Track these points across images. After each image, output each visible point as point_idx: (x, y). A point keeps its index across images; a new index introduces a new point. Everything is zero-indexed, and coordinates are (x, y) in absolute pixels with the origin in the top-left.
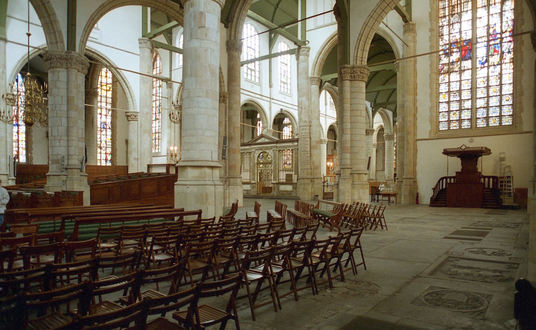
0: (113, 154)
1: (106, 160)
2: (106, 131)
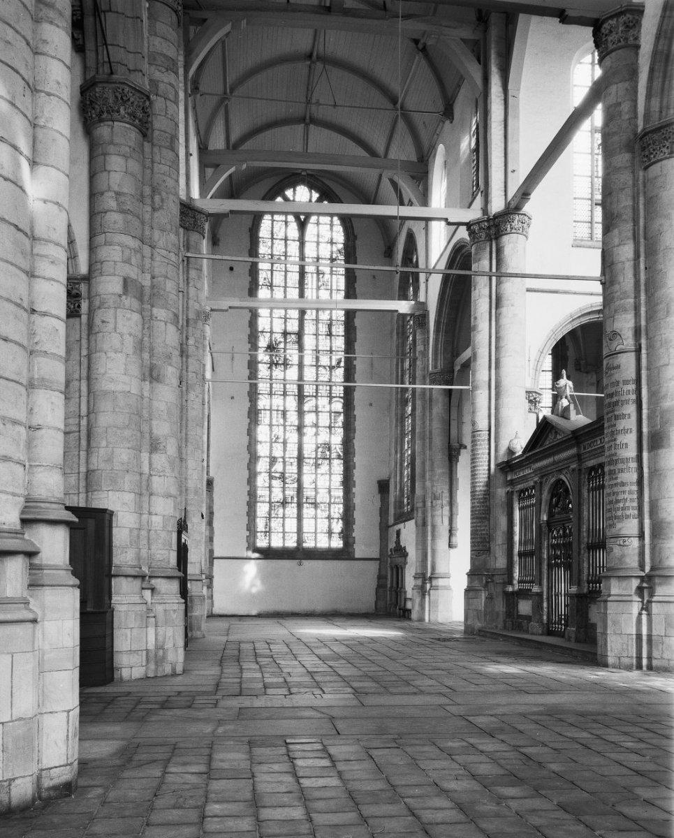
0: (348, 518)
1: (330, 533)
2: (330, 464)
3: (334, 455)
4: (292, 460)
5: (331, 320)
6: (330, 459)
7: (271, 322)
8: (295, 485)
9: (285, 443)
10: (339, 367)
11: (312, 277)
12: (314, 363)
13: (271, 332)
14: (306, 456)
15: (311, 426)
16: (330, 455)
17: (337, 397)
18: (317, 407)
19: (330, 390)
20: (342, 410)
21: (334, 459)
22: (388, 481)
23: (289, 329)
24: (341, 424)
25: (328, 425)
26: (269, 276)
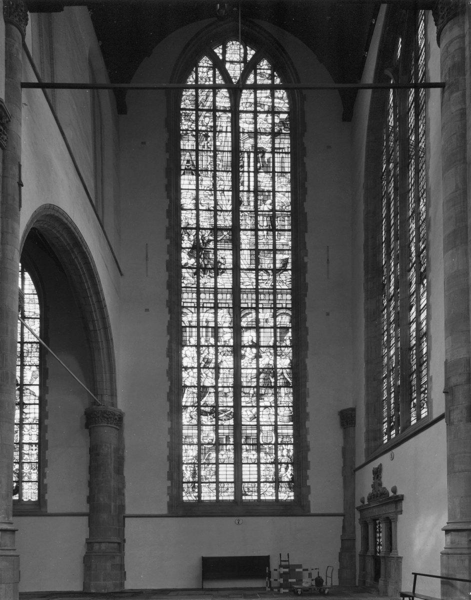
0: (299, 462)
1: (277, 482)
2: (276, 394)
3: (280, 382)
4: (226, 390)
5: (274, 210)
6: (275, 387)
7: (198, 216)
8: (231, 422)
9: (217, 368)
10: (287, 270)
11: (249, 157)
12: (253, 266)
13: (198, 228)
14: (244, 384)
15: (251, 346)
16: (276, 382)
17: (282, 308)
18: (257, 320)
19: (275, 300)
20: (289, 325)
21: (280, 387)
22: (353, 410)
23: (220, 223)
24: (288, 343)
25: (271, 344)
26: (194, 158)
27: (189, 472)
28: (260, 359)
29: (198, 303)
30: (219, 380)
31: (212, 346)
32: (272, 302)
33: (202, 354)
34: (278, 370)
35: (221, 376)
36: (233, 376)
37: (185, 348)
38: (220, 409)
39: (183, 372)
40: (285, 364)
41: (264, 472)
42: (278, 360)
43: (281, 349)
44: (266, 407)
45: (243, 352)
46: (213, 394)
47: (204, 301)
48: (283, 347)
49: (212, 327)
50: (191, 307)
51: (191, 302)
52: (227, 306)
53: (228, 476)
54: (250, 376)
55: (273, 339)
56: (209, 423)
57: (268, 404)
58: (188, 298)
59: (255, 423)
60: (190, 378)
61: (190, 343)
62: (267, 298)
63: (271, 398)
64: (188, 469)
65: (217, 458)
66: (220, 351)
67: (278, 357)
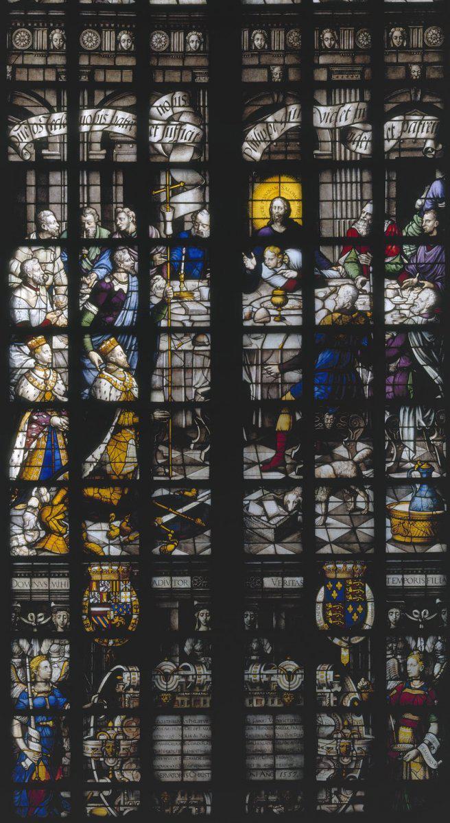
4: (184, 420)
8: (203, 545)
14: (256, 392)
15: (282, 243)
16: (378, 384)
17: (408, 83)
18: (307, 132)
27: (35, 746)
28: (320, 292)
29: (72, 67)
30: (157, 380)
31: (126, 241)
32: (367, 59)
33: (87, 273)
34: (388, 336)
35: (162, 361)
36: (208, 363)
37: (23, 253)
38: (158, 493)
39: (13, 348)
40: (415, 310)
41: (332, 744)
42: (389, 293)
43: (400, 252)
44: (337, 485)
45: (250, 263)
46: (128, 435)
47: (95, 61)
48: (410, 240)
49: (125, 166)
50: (45, 85)
51: (45, 67)
52: (188, 78)
53: (187, 761)
54: (275, 359)
55: (368, 208)
56: (115, 551)
57: (347, 469)
58: (32, 49)
59: (298, 547)
60: (40, 373)
61: (39, 230)
62: (348, 43)
63: (360, 446)
64: (33, 732)
65: (146, 685)
66: (159, 259)
67: (391, 285)
